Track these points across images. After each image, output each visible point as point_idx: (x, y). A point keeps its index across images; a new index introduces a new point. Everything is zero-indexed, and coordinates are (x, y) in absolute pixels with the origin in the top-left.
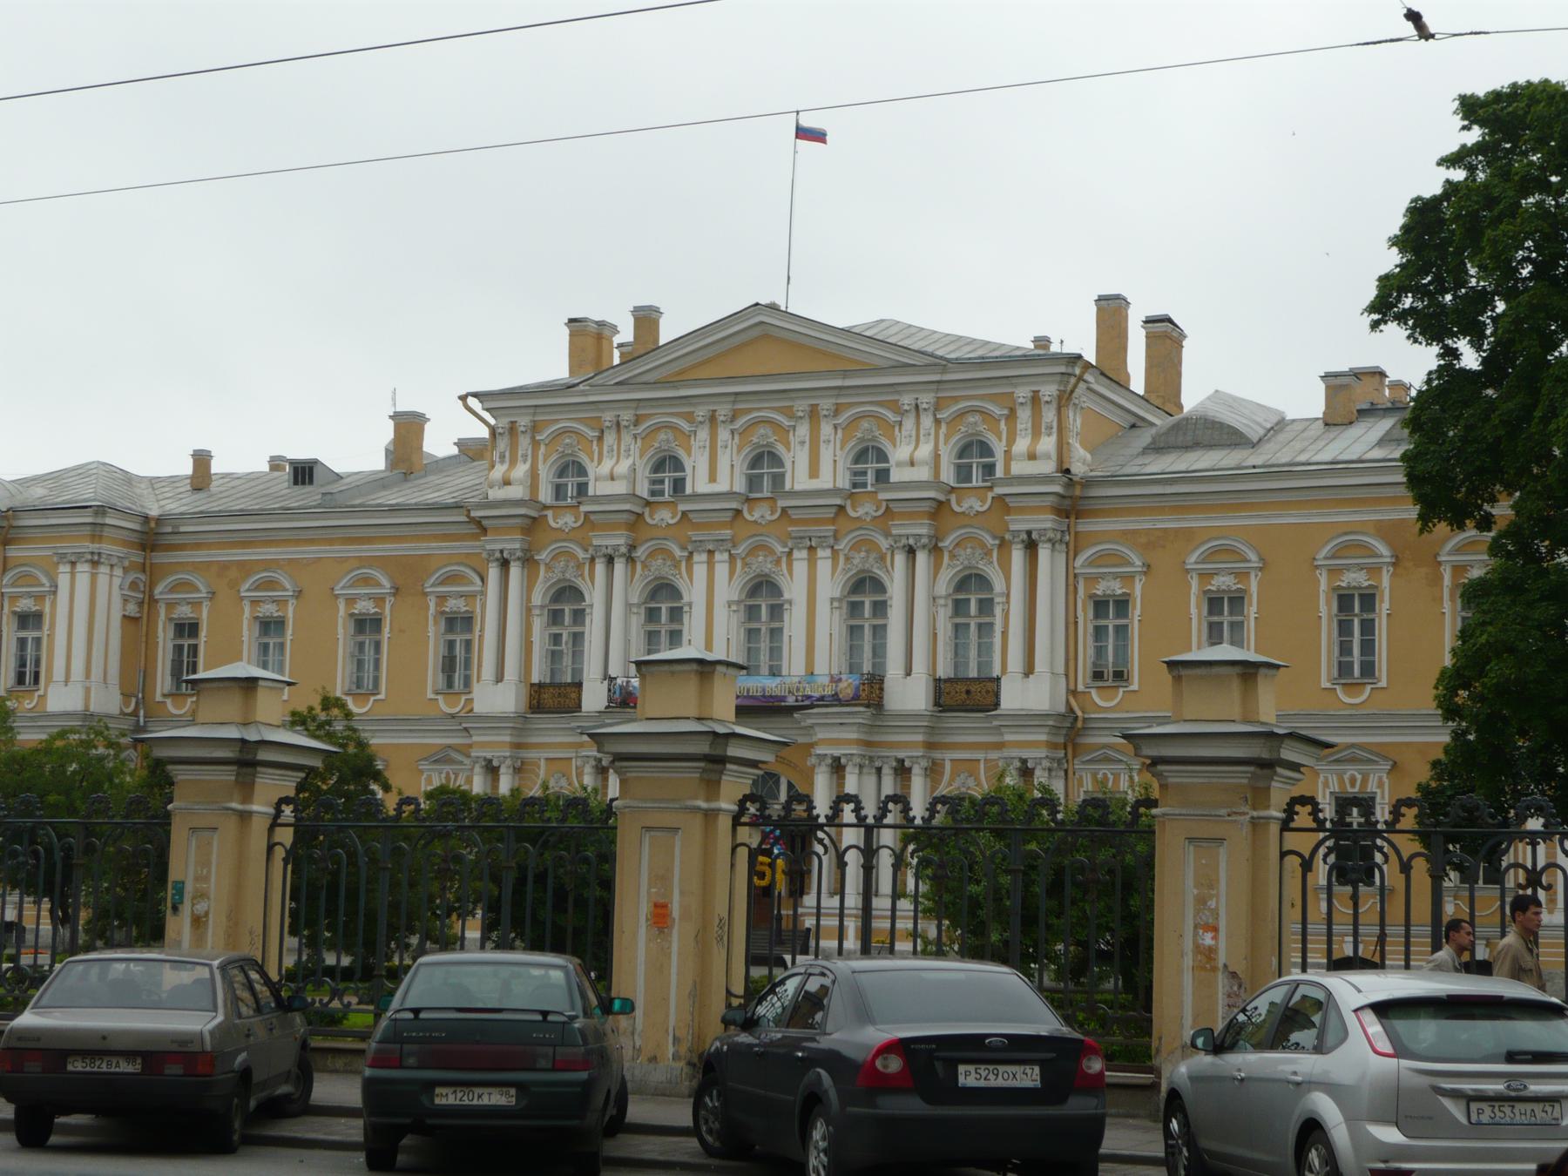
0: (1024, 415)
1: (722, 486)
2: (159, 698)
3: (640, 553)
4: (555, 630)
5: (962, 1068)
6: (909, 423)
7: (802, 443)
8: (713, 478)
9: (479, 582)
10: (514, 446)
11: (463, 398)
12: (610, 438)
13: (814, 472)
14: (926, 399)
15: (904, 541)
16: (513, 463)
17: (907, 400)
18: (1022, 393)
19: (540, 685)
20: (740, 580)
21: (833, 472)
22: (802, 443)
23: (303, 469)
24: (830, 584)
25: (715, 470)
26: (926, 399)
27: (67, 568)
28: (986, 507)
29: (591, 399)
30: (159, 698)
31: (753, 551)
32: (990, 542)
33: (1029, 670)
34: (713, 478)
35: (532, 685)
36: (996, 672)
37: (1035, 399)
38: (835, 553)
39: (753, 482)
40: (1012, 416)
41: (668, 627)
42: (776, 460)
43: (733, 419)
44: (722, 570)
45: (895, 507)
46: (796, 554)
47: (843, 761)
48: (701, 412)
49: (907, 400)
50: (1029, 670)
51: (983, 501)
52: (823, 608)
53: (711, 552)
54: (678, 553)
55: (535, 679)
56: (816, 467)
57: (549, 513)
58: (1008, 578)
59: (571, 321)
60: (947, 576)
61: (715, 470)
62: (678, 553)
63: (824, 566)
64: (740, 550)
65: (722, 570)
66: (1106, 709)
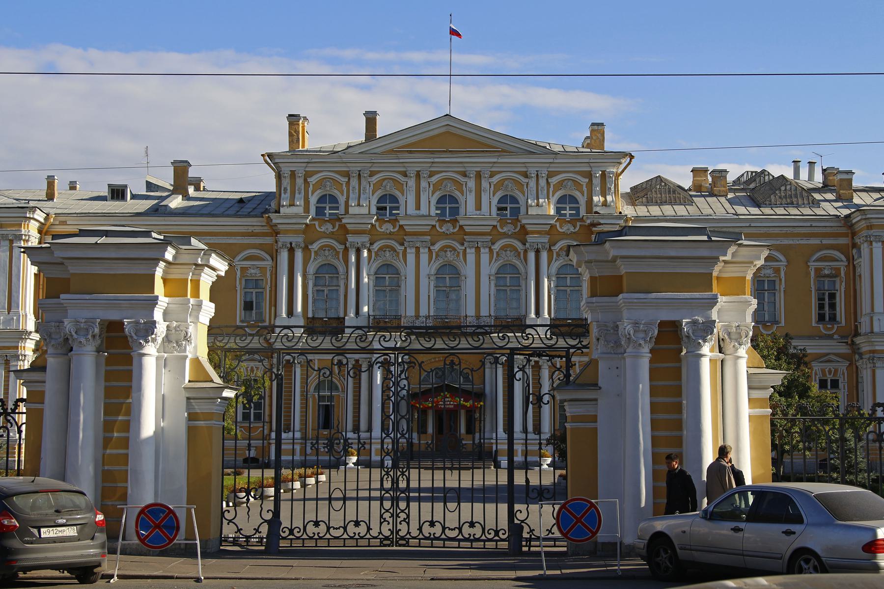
0: (597, 181)
1: (424, 210)
4: (319, 288)
5: (42, 530)
8: (418, 207)
9: (269, 258)
11: (262, 155)
12: (354, 182)
19: (313, 318)
22: (471, 191)
23: (118, 190)
28: (577, 229)
29: (401, 161)
31: (443, 249)
34: (418, 207)
35: (308, 318)
38: (491, 250)
42: (453, 200)
43: (430, 176)
44: (424, 257)
45: (529, 228)
49: (532, 171)
51: (575, 227)
52: (484, 280)
55: (310, 315)
57: (317, 223)
59: (290, 115)
60: (556, 265)
64: (437, 247)
65: (424, 257)
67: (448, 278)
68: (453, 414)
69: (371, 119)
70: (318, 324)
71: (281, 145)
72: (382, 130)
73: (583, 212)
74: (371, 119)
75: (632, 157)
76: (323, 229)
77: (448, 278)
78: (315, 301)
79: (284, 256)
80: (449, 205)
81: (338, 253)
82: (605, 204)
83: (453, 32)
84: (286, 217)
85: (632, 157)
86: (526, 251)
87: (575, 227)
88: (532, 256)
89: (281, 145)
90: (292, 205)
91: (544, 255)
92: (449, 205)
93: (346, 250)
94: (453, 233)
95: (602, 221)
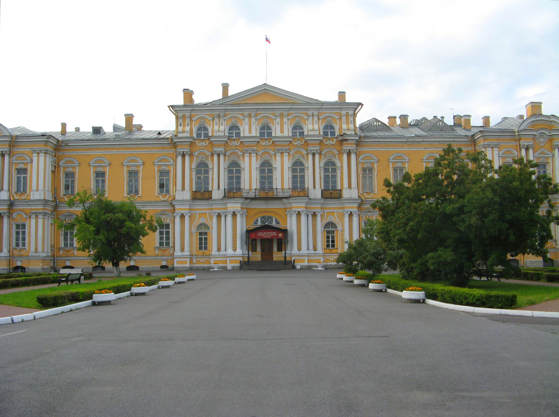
0: (344, 118)
1: (253, 134)
2: (62, 196)
3: (228, 153)
4: (199, 176)
6: (310, 119)
7: (278, 123)
8: (250, 132)
10: (184, 122)
12: (216, 120)
13: (282, 131)
14: (316, 113)
15: (313, 151)
16: (184, 126)
17: (310, 113)
18: (344, 112)
19: (196, 191)
20: (259, 162)
21: (287, 132)
22: (278, 123)
24: (288, 163)
25: (249, 129)
26: (316, 113)
27: (36, 155)
30: (62, 196)
32: (336, 152)
33: (350, 187)
34: (250, 132)
36: (339, 187)
37: (347, 114)
39: (262, 134)
40: (340, 118)
41: (266, 176)
46: (277, 154)
47: (317, 213)
48: (246, 113)
50: (350, 187)
53: (250, 153)
54: (240, 153)
56: (282, 130)
57: (197, 141)
58: (342, 163)
60: (323, 161)
61: (249, 129)
62: (240, 153)
63: (286, 158)
66: (369, 198)
67: (266, 169)
68: (270, 241)
69: (225, 87)
70: (198, 195)
71: (180, 101)
72: (231, 92)
73: (337, 134)
74: (225, 87)
75: (362, 105)
76: (200, 144)
77: (266, 169)
78: (197, 183)
79: (180, 159)
80: (265, 130)
81: (207, 157)
82: (348, 129)
83: (267, 40)
84: (181, 138)
85: (362, 105)
86: (307, 154)
87: (333, 142)
88: (310, 157)
89: (180, 101)
90: (183, 132)
91: (317, 156)
92: (265, 130)
93: (212, 155)
94: (269, 145)
95: (348, 138)
